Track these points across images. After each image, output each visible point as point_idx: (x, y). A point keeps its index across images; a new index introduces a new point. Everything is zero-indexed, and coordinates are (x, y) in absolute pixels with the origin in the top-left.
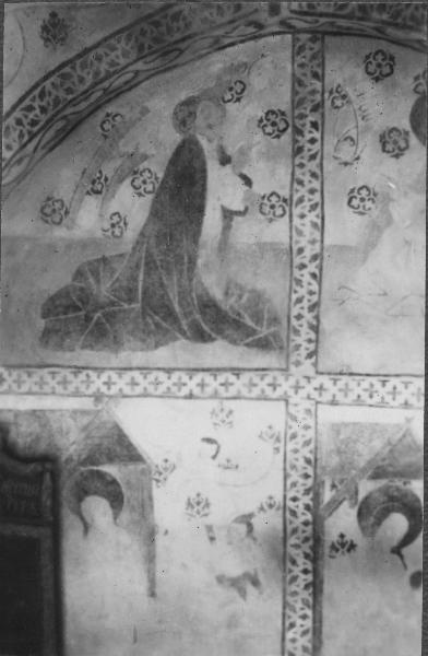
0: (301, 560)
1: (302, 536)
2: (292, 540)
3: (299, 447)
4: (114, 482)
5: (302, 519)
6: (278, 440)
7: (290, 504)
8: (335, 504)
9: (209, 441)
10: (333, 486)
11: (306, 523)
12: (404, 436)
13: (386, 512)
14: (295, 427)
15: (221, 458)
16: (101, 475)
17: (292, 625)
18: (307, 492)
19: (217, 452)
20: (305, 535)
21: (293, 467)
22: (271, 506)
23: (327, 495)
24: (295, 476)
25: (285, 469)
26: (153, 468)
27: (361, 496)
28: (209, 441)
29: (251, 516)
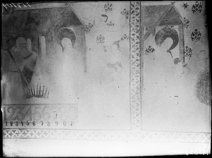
0: (135, 56)
1: (136, 48)
2: (132, 50)
3: (135, 16)
4: (72, 32)
5: (136, 41)
6: (128, 14)
7: (132, 36)
8: (148, 35)
9: (103, 15)
10: (147, 29)
11: (137, 43)
12: (171, 9)
13: (165, 37)
14: (134, 9)
15: (108, 22)
16: (68, 30)
17: (133, 80)
18: (137, 32)
19: (107, 20)
20: (137, 47)
21: (133, 23)
22: (125, 38)
23: (145, 32)
24: (133, 26)
25: (130, 24)
26: (85, 26)
27: (156, 32)
28: (103, 15)
29: (119, 41)
